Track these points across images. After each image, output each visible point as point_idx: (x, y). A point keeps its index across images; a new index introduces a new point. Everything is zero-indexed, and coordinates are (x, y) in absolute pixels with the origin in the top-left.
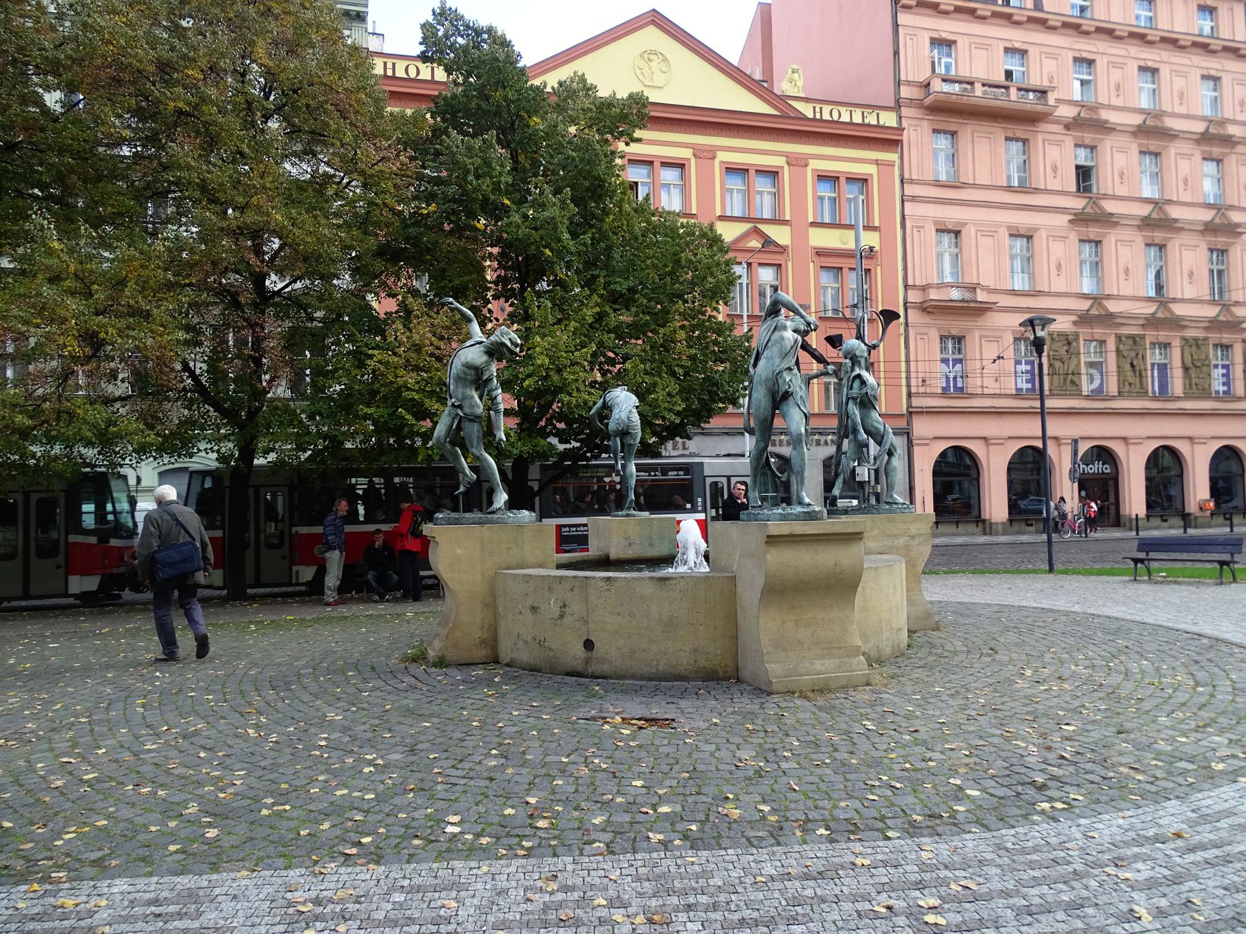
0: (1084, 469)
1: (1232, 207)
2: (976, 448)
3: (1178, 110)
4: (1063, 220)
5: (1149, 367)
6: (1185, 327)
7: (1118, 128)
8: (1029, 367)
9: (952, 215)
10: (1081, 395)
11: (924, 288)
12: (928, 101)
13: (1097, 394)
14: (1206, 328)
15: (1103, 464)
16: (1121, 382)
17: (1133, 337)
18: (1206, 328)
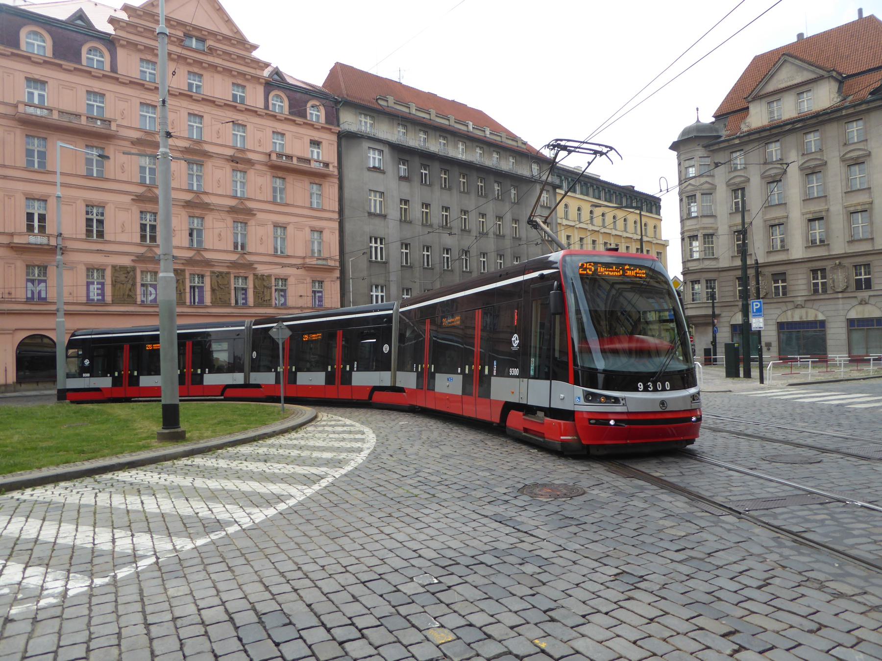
1: (249, 199)
3: (215, 141)
4: (127, 199)
5: (188, 290)
6: (213, 266)
8: (100, 286)
9: (38, 190)
12: (269, 163)
13: (143, 304)
14: (228, 267)
18: (228, 267)
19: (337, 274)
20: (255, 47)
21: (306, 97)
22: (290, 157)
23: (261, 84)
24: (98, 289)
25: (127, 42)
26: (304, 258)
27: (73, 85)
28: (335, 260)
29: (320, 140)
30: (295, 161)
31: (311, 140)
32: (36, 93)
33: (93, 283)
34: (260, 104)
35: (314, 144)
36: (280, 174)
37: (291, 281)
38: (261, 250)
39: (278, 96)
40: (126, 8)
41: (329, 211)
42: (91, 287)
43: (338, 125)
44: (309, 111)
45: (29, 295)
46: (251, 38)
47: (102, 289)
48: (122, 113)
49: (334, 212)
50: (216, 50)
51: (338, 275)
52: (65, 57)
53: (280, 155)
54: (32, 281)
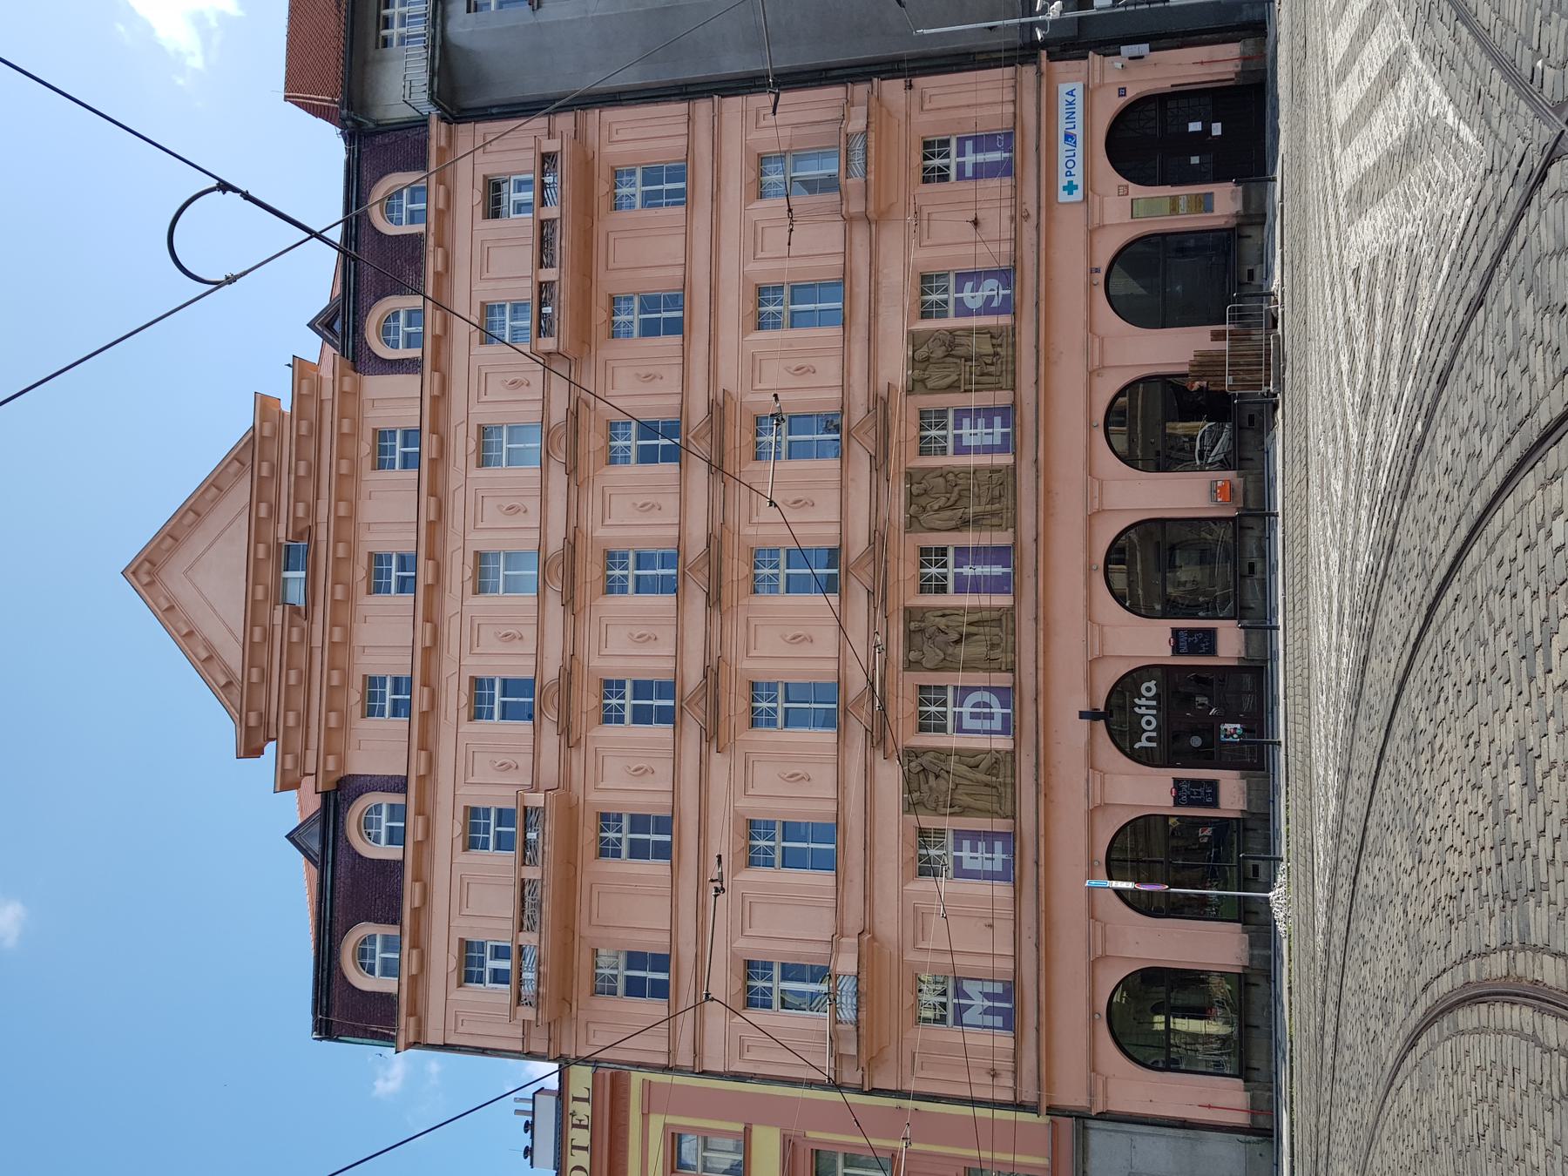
0: (1149, 739)
2: (1110, 978)
7: (569, 652)
8: (966, 844)
9: (724, 981)
10: (1013, 752)
11: (838, 1058)
15: (1140, 696)
16: (990, 665)
17: (909, 635)
19: (893, 89)
20: (264, 405)
21: (365, 238)
22: (544, 290)
23: (357, 392)
24: (974, 849)
25: (328, 753)
26: (848, 220)
27: (456, 881)
28: (849, 102)
29: (480, 184)
30: (548, 275)
31: (486, 216)
32: (491, 964)
33: (958, 860)
34: (407, 384)
35: (498, 201)
36: (600, 314)
37: (927, 258)
38: (829, 370)
39: (386, 332)
40: (250, 749)
41: (690, 136)
42: (967, 865)
43: (423, 123)
44: (406, 229)
45: (999, 1021)
46: (240, 422)
47: (975, 836)
48: (504, 767)
49: (690, 119)
50: (296, 519)
51: (901, 82)
52: (397, 897)
53: (543, 327)
54: (960, 1010)
